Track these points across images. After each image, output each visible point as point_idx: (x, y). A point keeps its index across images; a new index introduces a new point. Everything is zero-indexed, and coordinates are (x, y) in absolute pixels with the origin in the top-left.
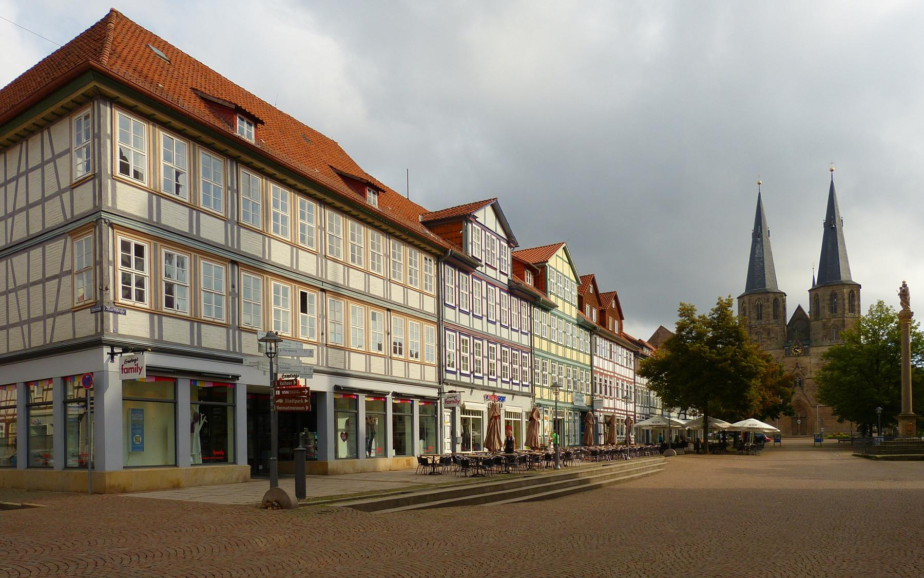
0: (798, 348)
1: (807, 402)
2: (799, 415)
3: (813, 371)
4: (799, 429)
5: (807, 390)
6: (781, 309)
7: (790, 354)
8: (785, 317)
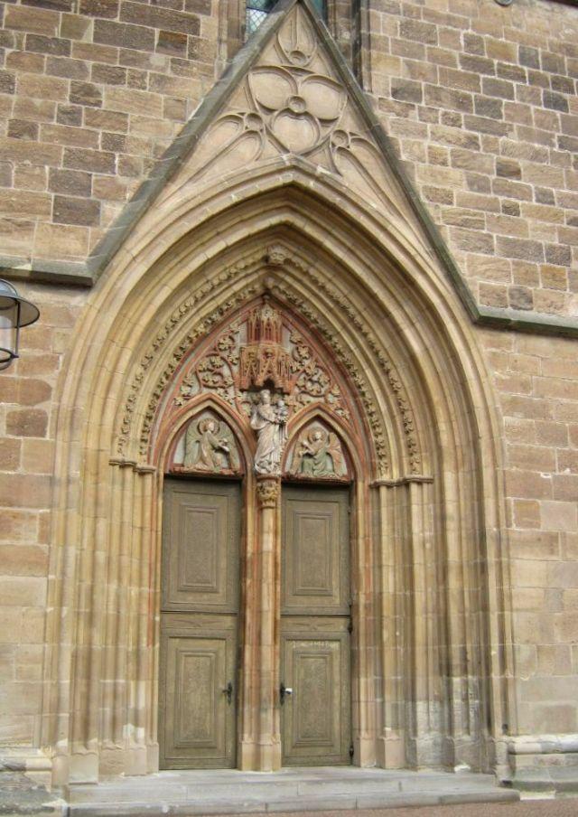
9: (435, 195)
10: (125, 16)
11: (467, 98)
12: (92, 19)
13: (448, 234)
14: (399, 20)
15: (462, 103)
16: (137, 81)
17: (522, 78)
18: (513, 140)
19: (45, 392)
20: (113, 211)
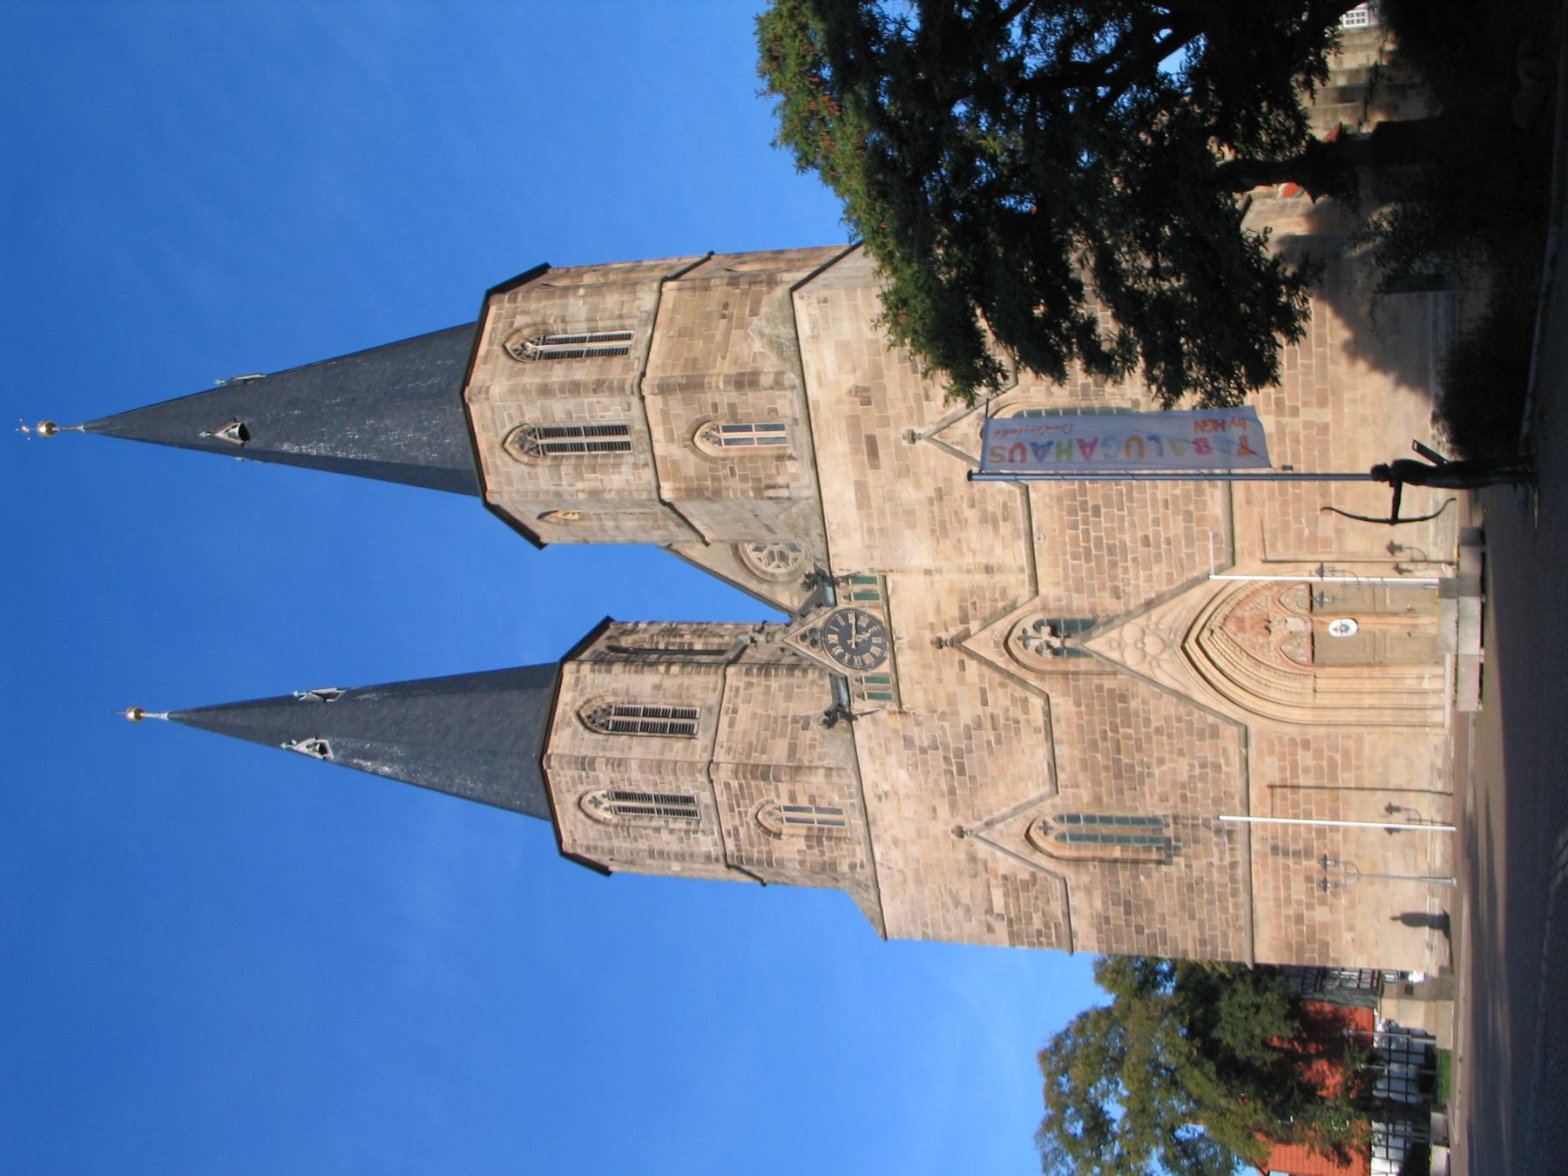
3: (982, 560)
5: (1116, 593)
7: (882, 679)
10: (1116, 716)
11: (1109, 562)
12: (1121, 730)
14: (1075, 596)
15: (1114, 564)
16: (1147, 712)
17: (1086, 532)
18: (1127, 538)
20: (1211, 719)
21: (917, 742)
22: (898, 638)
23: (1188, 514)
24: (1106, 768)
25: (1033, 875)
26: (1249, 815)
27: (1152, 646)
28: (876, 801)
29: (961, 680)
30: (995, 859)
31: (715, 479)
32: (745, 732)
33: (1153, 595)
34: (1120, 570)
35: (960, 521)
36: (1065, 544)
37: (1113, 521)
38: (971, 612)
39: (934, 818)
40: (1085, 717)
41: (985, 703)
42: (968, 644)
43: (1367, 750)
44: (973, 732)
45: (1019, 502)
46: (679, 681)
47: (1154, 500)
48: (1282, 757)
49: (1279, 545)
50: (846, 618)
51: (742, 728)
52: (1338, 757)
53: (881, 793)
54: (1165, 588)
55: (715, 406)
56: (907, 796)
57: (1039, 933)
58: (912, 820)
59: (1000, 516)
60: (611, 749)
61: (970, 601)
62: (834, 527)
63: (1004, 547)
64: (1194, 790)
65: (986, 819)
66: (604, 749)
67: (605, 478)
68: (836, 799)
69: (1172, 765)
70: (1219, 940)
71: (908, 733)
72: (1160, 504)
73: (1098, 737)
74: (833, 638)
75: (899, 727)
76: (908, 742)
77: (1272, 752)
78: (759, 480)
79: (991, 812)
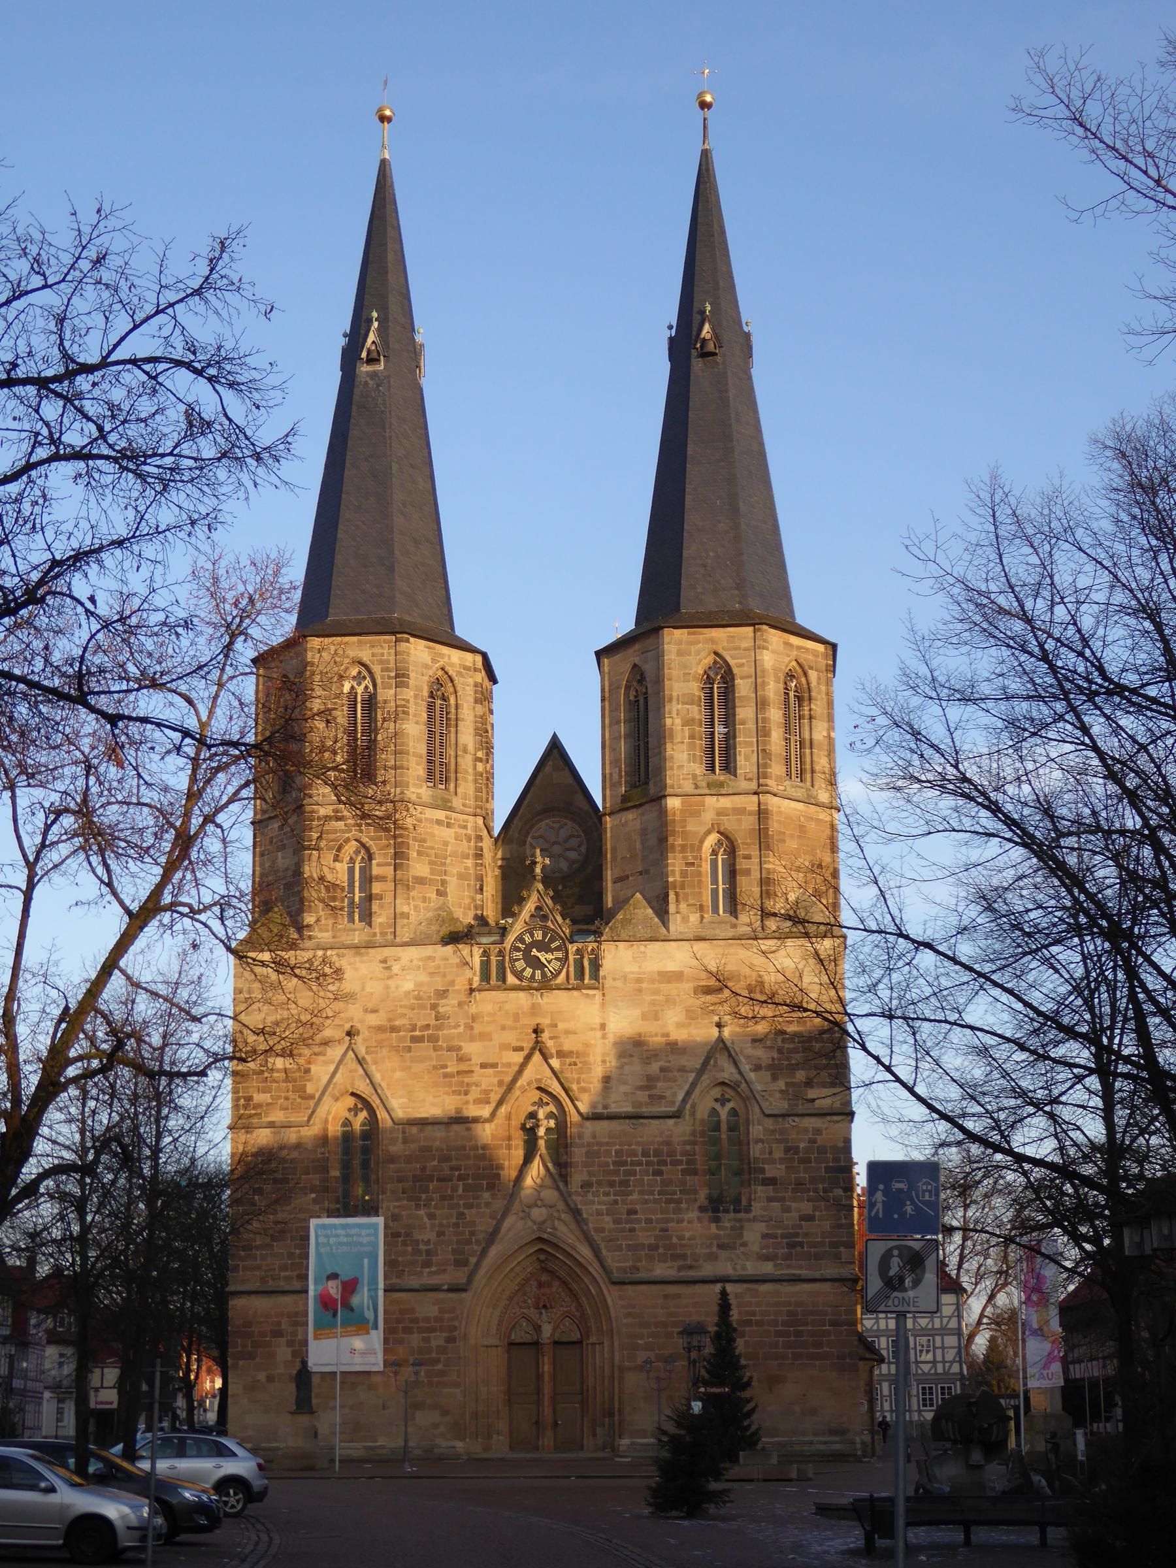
0: (543, 947)
1: (585, 1252)
2: (547, 1330)
4: (547, 1410)
5: (586, 1185)
6: (467, 736)
8: (486, 781)
9: (597, 1230)
13: (603, 1245)
14: (584, 1150)
15: (611, 1184)
16: (478, 1207)
17: (640, 1164)
18: (635, 1196)
19: (455, 1328)
20: (473, 1260)
21: (442, 1002)
22: (542, 995)
23: (656, 1247)
24: (424, 1169)
25: (312, 1097)
26: (385, 1291)
27: (538, 1213)
28: (379, 957)
29: (504, 1047)
30: (326, 1063)
31: (684, 848)
32: (433, 835)
33: (585, 1216)
34: (607, 1189)
35: (648, 1058)
36: (629, 1145)
37: (649, 1185)
38: (568, 1061)
39: (366, 1011)
40: (472, 1153)
41: (483, 1066)
42: (537, 1057)
43: (446, 1390)
44: (454, 1054)
45: (663, 1109)
46: (471, 770)
47: (668, 1221)
48: (437, 1319)
49: (630, 1320)
50: (558, 949)
51: (436, 832)
52: (440, 1366)
53: (389, 964)
54: (591, 1225)
55: (748, 857)
56: (387, 987)
57: (249, 1099)
58: (363, 989)
59: (652, 1092)
60: (416, 704)
61: (577, 1061)
62: (642, 948)
63: (626, 1094)
64: (404, 1244)
65: (368, 1058)
66: (416, 696)
67: (685, 747)
68: (380, 920)
69: (428, 1226)
70: (249, 1263)
71: (451, 995)
72: (663, 1225)
73: (454, 1163)
74: (538, 935)
75: (456, 987)
76: (442, 994)
77: (442, 1311)
78: (683, 887)
79: (375, 1063)
